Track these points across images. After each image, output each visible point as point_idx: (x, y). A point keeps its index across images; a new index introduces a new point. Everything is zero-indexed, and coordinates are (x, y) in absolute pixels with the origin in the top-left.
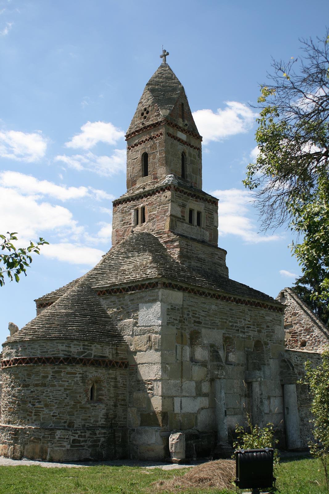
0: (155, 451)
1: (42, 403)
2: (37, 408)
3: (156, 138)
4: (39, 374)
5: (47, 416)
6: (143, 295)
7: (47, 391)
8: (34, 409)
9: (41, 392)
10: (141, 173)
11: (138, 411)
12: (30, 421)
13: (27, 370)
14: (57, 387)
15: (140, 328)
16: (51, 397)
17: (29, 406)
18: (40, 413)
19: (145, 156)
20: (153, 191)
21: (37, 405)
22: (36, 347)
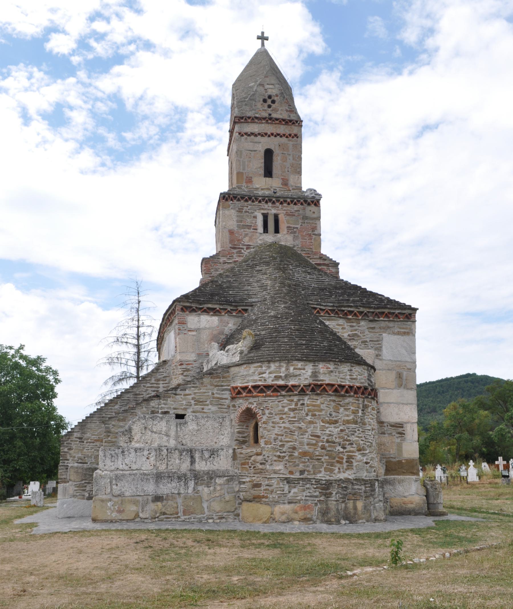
0: (414, 503)
1: (354, 446)
2: (350, 452)
3: (287, 137)
4: (349, 407)
5: (360, 463)
6: (391, 324)
7: (359, 430)
8: (346, 454)
9: (353, 431)
10: (262, 172)
11: (383, 458)
12: (341, 470)
13: (334, 401)
14: (367, 425)
15: (385, 362)
16: (363, 439)
17: (339, 450)
18: (353, 459)
19: (269, 154)
20: (292, 199)
21: (349, 448)
22: (345, 371)
